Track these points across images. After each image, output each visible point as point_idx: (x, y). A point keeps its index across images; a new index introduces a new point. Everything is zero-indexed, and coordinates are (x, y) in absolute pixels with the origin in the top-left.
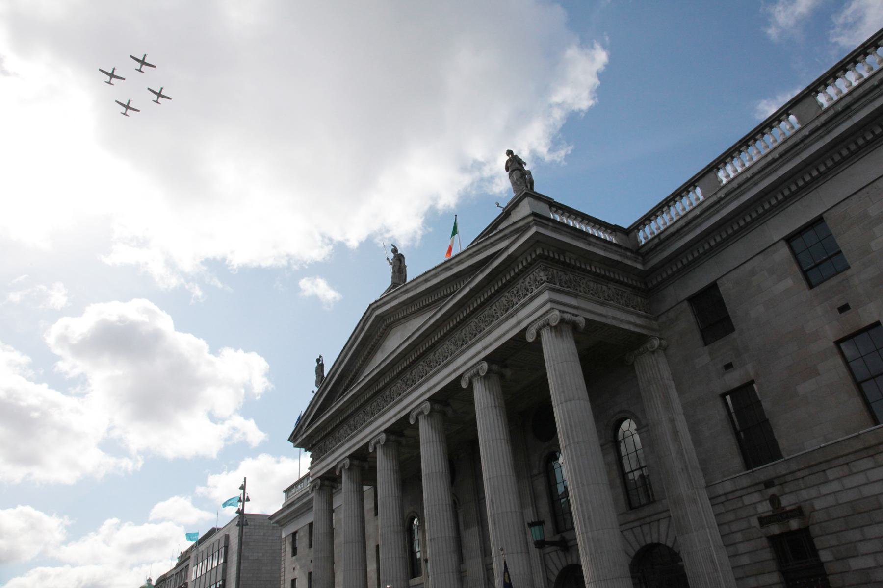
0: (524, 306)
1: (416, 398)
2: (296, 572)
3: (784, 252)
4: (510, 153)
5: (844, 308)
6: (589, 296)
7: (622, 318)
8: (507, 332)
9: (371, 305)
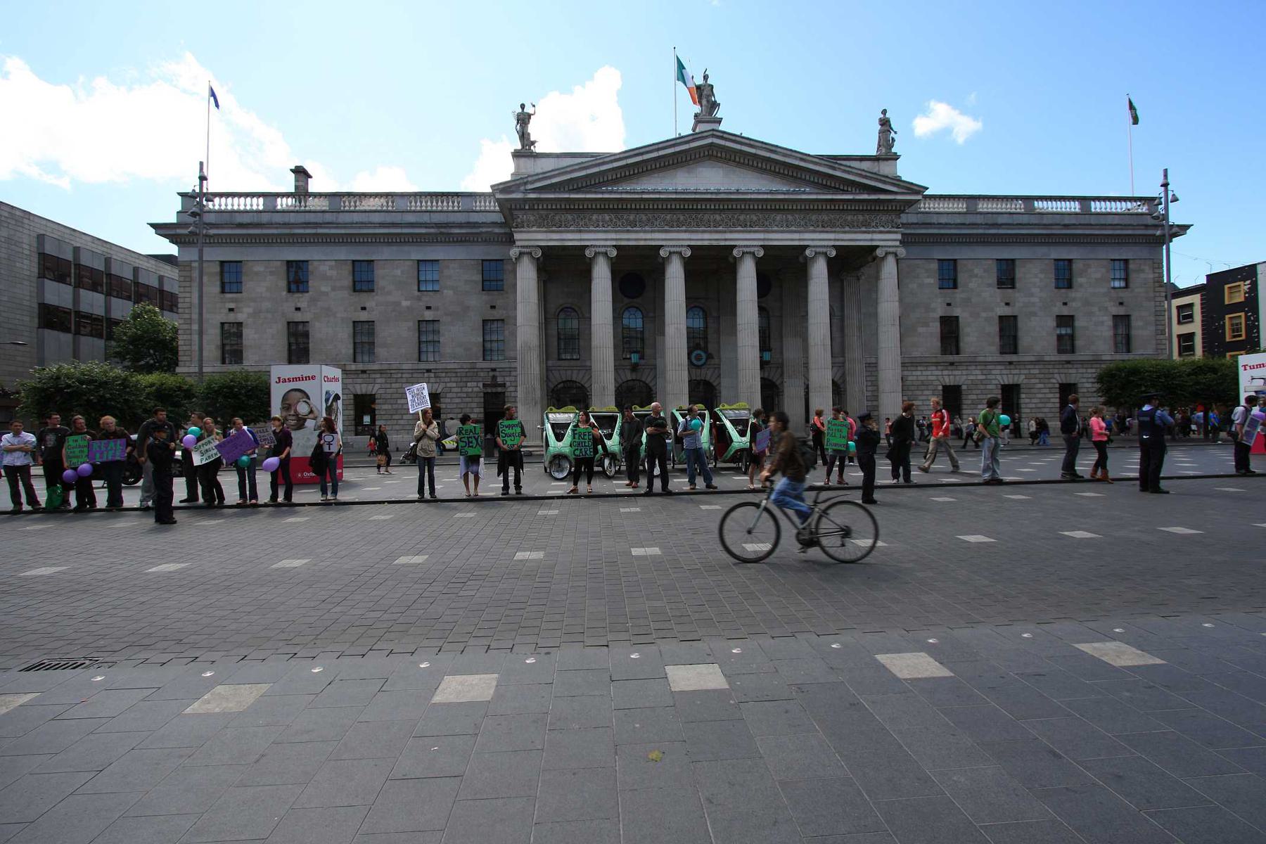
0: (881, 232)
1: (748, 240)
2: (216, 316)
3: (935, 266)
4: (884, 112)
5: (949, 304)
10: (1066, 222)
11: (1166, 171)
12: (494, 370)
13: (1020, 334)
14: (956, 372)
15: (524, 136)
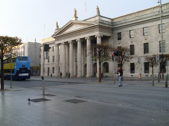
5: (132, 42)
6: (104, 32)
7: (108, 34)
10: (155, 14)
13: (149, 48)
14: (133, 60)
15: (58, 26)
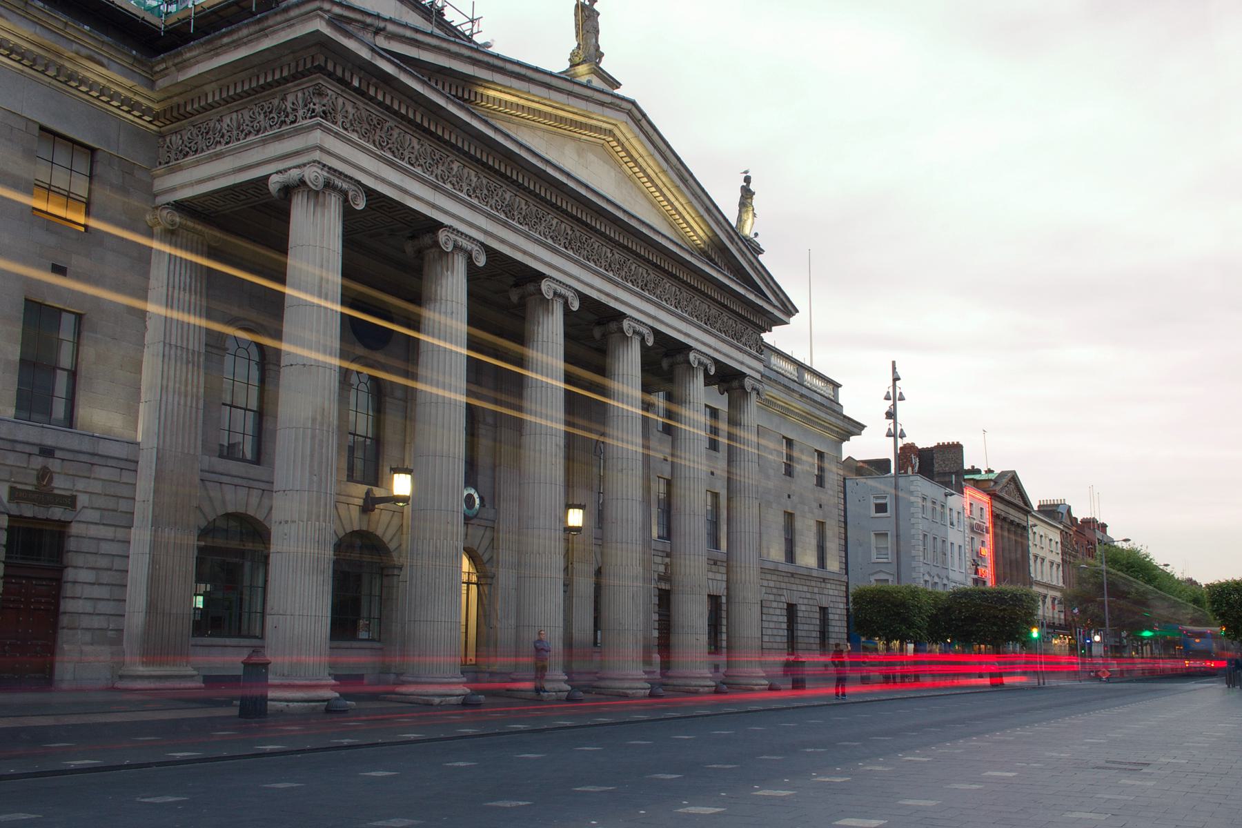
8: (731, 358)
9: (633, 103)
11: (894, 363)
12: (47, 452)
